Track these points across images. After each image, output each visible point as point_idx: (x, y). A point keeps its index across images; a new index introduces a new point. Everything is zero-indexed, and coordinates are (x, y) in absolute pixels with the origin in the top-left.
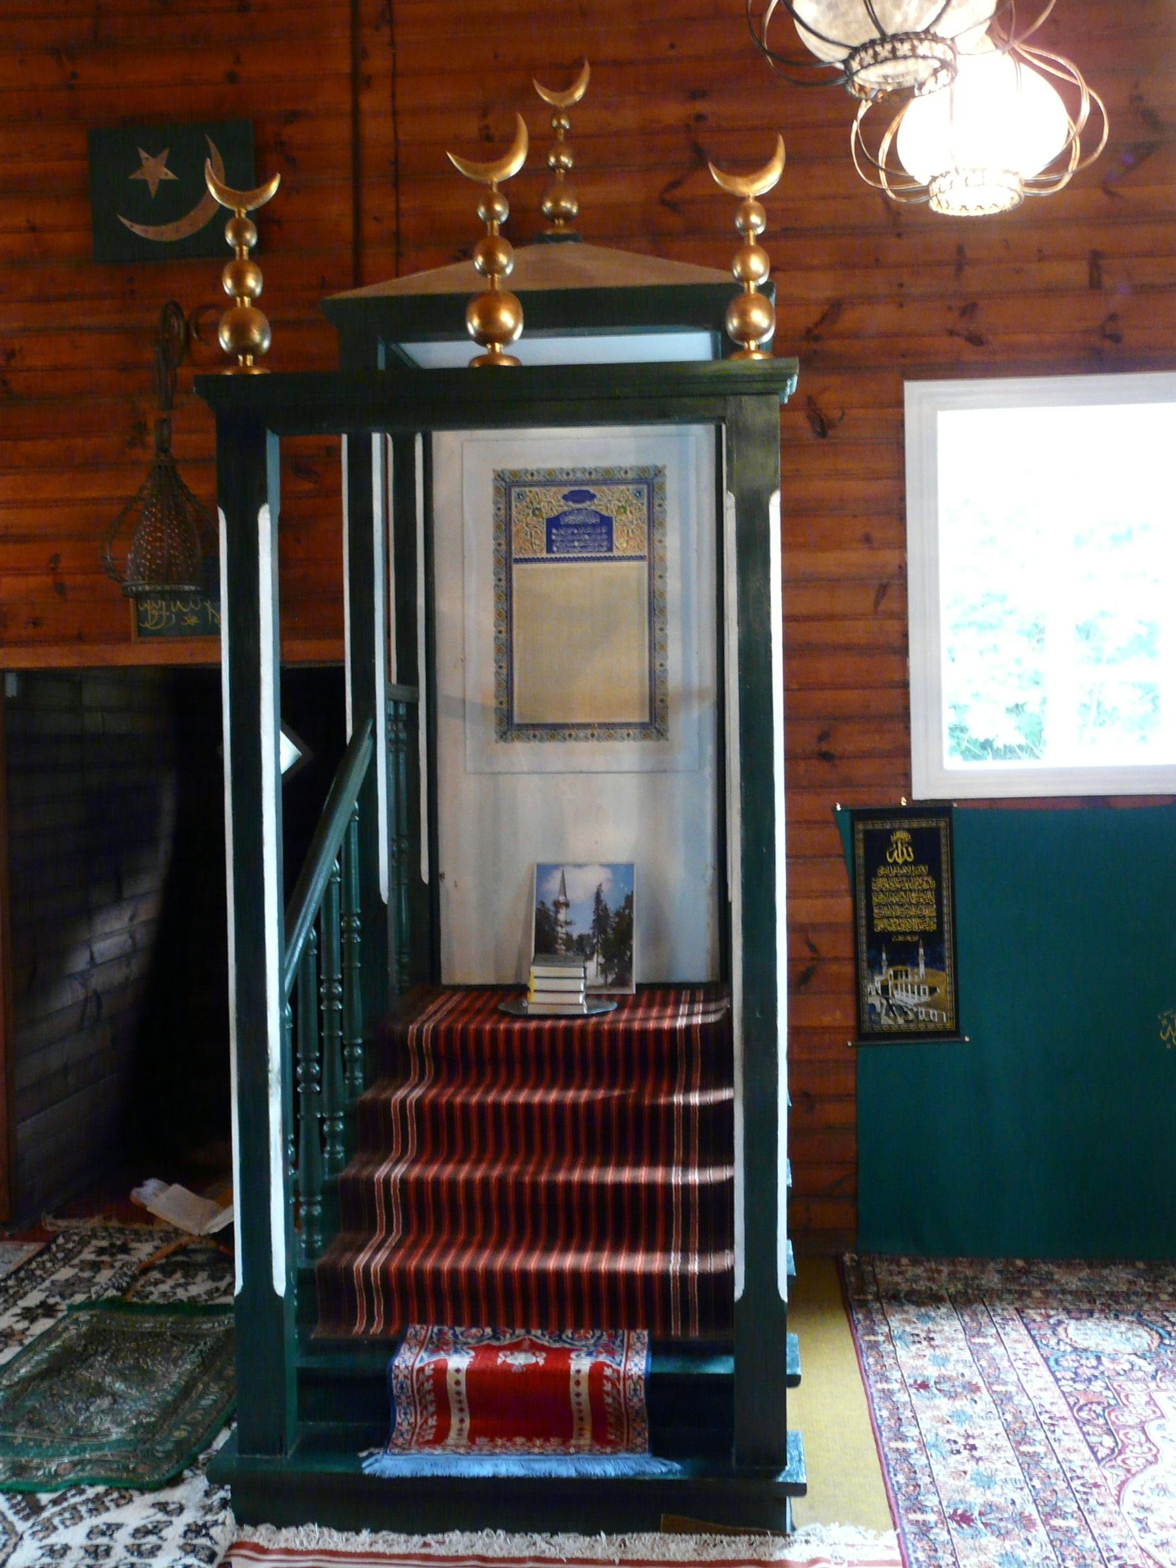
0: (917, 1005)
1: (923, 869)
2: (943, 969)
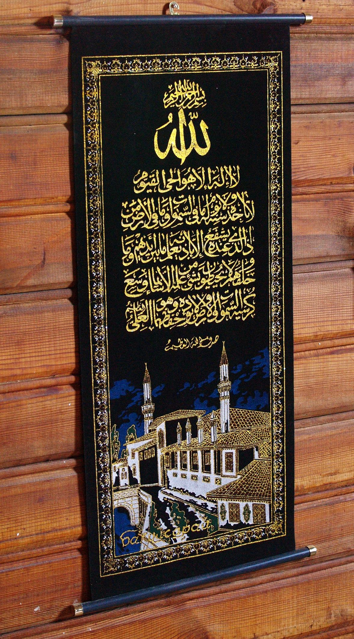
0: (211, 497)
1: (230, 174)
2: (267, 409)
